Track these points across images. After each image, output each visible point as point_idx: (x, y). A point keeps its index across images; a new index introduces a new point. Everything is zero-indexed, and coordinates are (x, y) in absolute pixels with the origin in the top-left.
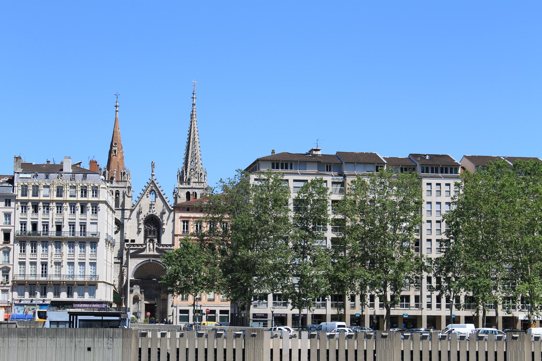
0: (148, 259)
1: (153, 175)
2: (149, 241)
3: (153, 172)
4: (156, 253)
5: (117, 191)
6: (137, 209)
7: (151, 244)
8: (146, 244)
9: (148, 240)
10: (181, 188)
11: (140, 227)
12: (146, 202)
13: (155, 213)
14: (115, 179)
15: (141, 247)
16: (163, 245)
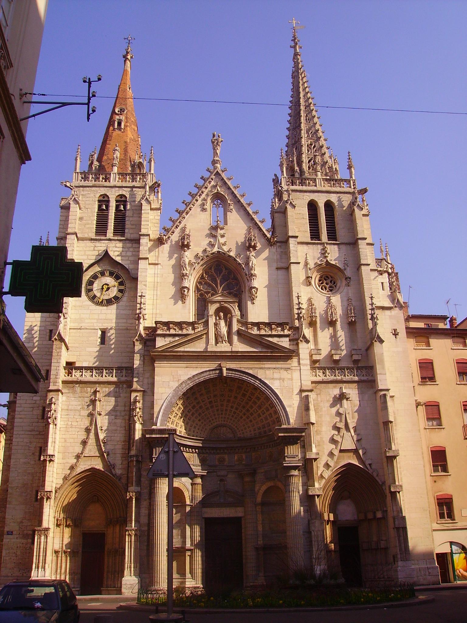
0: (213, 365)
1: (214, 162)
2: (217, 312)
3: (215, 154)
4: (239, 347)
5: (122, 196)
6: (175, 237)
7: (222, 323)
8: (206, 324)
9: (212, 309)
11: (186, 284)
12: (198, 222)
13: (226, 249)
14: (115, 169)
15: (190, 331)
16: (258, 325)
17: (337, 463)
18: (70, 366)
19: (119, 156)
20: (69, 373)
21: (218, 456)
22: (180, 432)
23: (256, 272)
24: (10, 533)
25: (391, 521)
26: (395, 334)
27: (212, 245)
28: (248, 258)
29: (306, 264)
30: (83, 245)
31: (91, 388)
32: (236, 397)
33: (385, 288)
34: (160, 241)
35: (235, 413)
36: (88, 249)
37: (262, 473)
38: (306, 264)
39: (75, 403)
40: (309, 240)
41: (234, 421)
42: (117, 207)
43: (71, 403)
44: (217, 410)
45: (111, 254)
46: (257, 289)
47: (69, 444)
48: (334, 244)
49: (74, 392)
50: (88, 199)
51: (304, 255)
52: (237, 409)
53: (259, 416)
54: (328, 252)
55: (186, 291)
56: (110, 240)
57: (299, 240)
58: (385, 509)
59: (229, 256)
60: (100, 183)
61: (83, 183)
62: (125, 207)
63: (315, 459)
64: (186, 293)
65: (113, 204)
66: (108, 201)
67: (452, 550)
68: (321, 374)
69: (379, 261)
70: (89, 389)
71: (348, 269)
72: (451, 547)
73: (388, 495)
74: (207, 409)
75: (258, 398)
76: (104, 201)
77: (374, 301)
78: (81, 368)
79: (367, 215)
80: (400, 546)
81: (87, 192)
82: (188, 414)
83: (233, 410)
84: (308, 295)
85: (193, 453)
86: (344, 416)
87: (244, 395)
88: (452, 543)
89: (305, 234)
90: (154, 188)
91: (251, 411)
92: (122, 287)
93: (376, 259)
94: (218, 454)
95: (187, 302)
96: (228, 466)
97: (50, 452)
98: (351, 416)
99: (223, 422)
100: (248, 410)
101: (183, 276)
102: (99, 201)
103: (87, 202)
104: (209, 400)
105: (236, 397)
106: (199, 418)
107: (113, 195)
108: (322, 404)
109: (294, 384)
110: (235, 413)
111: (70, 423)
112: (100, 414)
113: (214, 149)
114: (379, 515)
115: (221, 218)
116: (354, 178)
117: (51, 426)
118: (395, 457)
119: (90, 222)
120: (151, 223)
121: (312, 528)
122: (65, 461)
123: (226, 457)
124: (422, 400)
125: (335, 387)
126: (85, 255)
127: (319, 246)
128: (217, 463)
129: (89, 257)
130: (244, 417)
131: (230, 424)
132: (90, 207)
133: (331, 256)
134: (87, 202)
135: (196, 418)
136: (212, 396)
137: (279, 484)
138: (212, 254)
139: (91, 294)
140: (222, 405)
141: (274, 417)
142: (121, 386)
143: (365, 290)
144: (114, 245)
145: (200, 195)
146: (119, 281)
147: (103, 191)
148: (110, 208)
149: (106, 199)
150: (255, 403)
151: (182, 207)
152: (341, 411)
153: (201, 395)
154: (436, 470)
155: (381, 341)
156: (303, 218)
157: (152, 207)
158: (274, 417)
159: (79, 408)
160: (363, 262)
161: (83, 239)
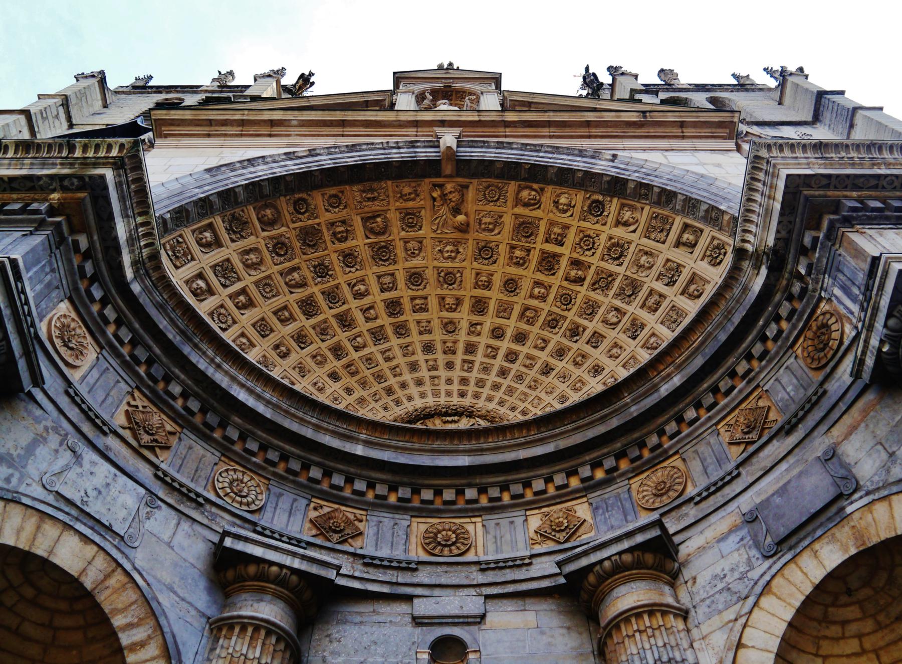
21: (420, 526)
37: (723, 538)
41: (510, 391)
52: (520, 338)
82: (274, 321)
83: (505, 345)
87: (549, 262)
99: (455, 400)
104: (387, 295)
105: (511, 285)
106: (334, 364)
110: (512, 356)
131: (492, 406)
135: (319, 359)
136: (401, 277)
140: (450, 327)
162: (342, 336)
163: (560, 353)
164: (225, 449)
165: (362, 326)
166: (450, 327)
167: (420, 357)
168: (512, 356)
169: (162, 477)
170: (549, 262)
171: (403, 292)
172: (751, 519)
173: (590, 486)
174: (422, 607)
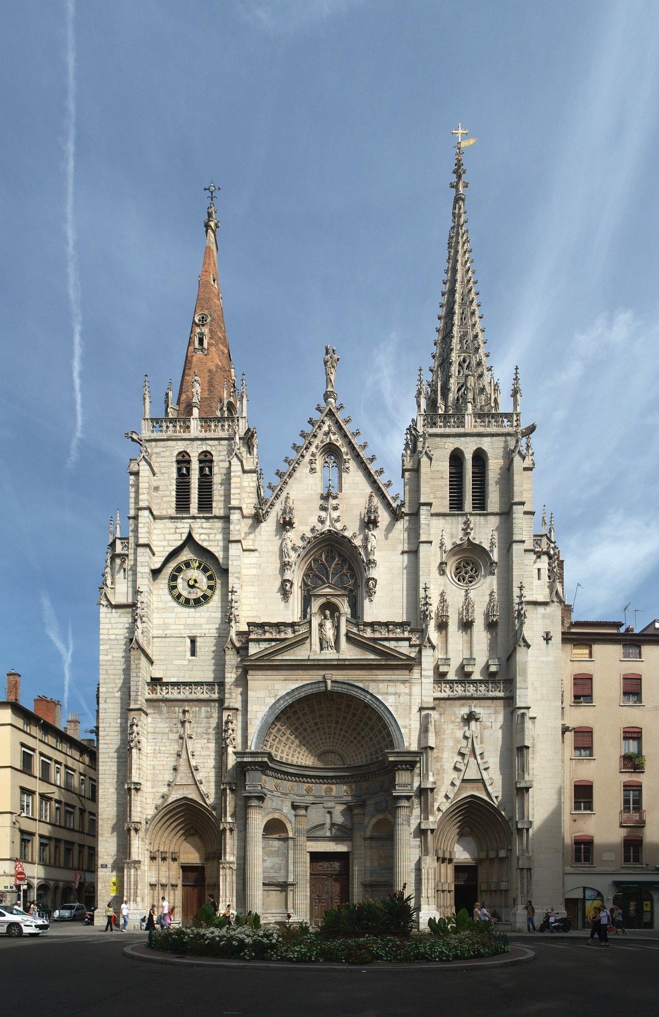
5: (206, 453)
10: (431, 435)
11: (288, 575)
13: (339, 526)
14: (196, 412)
17: (456, 794)
18: (156, 682)
19: (199, 391)
20: (153, 691)
21: (325, 786)
22: (281, 758)
23: (375, 558)
24: (104, 866)
25: (514, 861)
26: (547, 638)
27: (322, 522)
28: (366, 539)
29: (442, 544)
30: (162, 526)
31: (179, 707)
32: (345, 718)
33: (542, 576)
34: (258, 519)
35: (344, 736)
36: (167, 531)
38: (442, 544)
39: (162, 725)
40: (447, 511)
42: (201, 469)
43: (158, 725)
44: (325, 733)
45: (196, 537)
46: (376, 581)
47: (158, 772)
48: (480, 515)
49: (160, 713)
50: (163, 459)
51: (441, 532)
52: (346, 732)
53: (371, 740)
54: (471, 526)
55: (289, 585)
56: (194, 518)
57: (433, 511)
58: (510, 847)
59: (344, 537)
60: (178, 434)
61: (155, 435)
62: (211, 469)
63: (432, 790)
64: (288, 588)
65: (195, 466)
66: (189, 462)
67: (584, 896)
68: (447, 690)
69: (538, 538)
70: (177, 709)
71: (496, 550)
72: (584, 893)
73: (515, 832)
74: (313, 731)
75: (370, 719)
76: (183, 461)
77: (524, 592)
78: (167, 684)
79: (530, 469)
80: (522, 888)
81: (161, 449)
83: (343, 733)
84: (439, 586)
85: (296, 781)
86: (470, 740)
87: (354, 715)
88: (585, 888)
89: (442, 503)
90: (248, 439)
91: (363, 734)
92: (212, 583)
93: (535, 536)
94: (325, 783)
95: (291, 600)
96: (335, 797)
97: (135, 779)
98: (479, 741)
100: (359, 734)
101: (285, 565)
102: (178, 462)
103: (162, 464)
105: (345, 718)
107: (195, 453)
108: (445, 726)
109: (413, 701)
111: (157, 748)
112: (191, 738)
113: (327, 375)
114: (502, 854)
115: (335, 482)
116: (518, 411)
117: (134, 751)
118: (527, 789)
119: (168, 493)
120: (244, 492)
121: (423, 865)
122: (154, 790)
123: (334, 787)
124: (571, 724)
125: (463, 705)
126: (165, 539)
127: (460, 518)
128: (324, 794)
129: (171, 543)
130: (355, 742)
132: (166, 470)
133: (475, 533)
134: (162, 464)
137: (389, 817)
138: (322, 534)
139: (175, 592)
140: (330, 727)
141: (388, 740)
142: (213, 704)
143: (514, 579)
144: (199, 525)
145: (307, 448)
146: (209, 573)
147: (180, 446)
148: (192, 472)
149: (187, 457)
150: (366, 724)
151: (285, 468)
152: (467, 734)
153: (304, 714)
154: (577, 808)
155: (528, 646)
156: (442, 478)
157: (246, 468)
158: (388, 740)
159: (167, 730)
160: (516, 537)
161: (161, 518)
162: (305, 734)
163: (355, 738)
164: (289, 780)
165: (309, 730)
166: (330, 727)
167: (323, 736)
168: (344, 736)
169: (282, 794)
170: (354, 715)
171: (318, 720)
172: (376, 803)
173: (355, 782)
174: (325, 805)
